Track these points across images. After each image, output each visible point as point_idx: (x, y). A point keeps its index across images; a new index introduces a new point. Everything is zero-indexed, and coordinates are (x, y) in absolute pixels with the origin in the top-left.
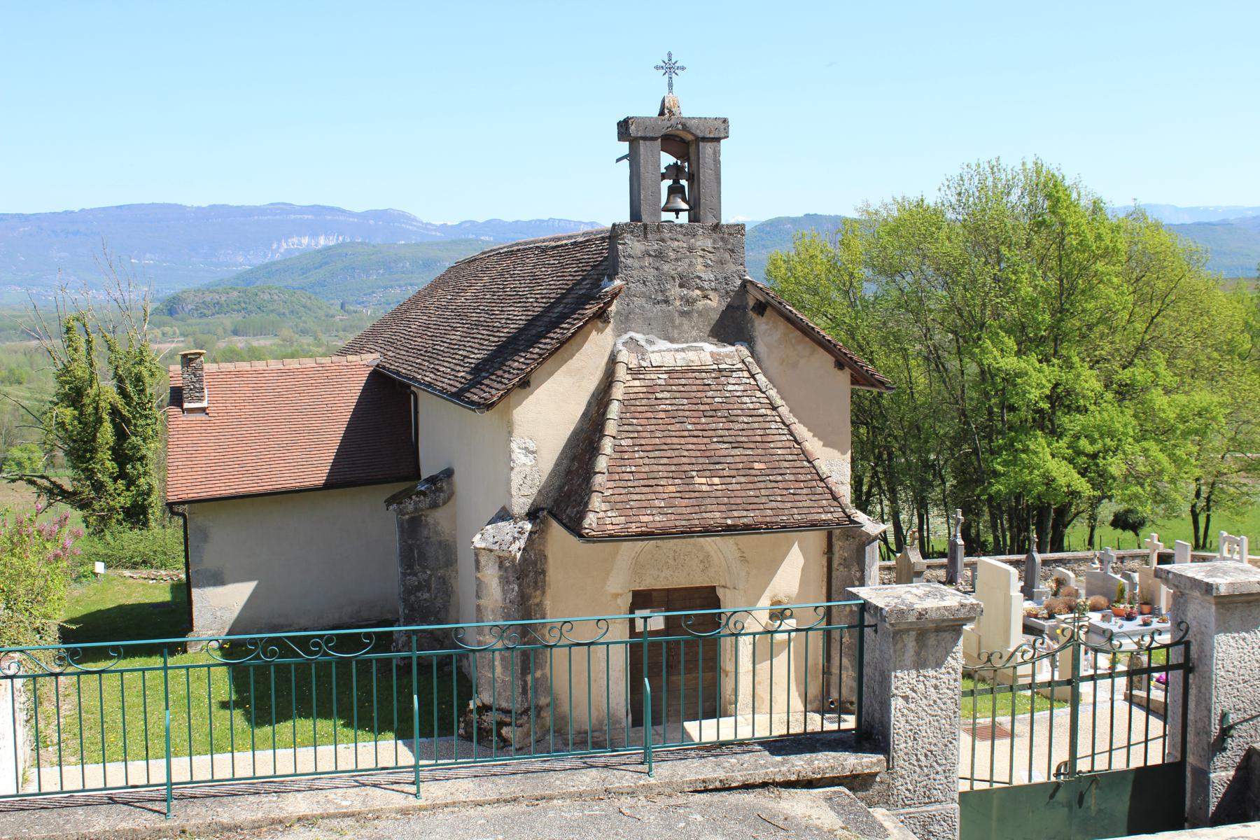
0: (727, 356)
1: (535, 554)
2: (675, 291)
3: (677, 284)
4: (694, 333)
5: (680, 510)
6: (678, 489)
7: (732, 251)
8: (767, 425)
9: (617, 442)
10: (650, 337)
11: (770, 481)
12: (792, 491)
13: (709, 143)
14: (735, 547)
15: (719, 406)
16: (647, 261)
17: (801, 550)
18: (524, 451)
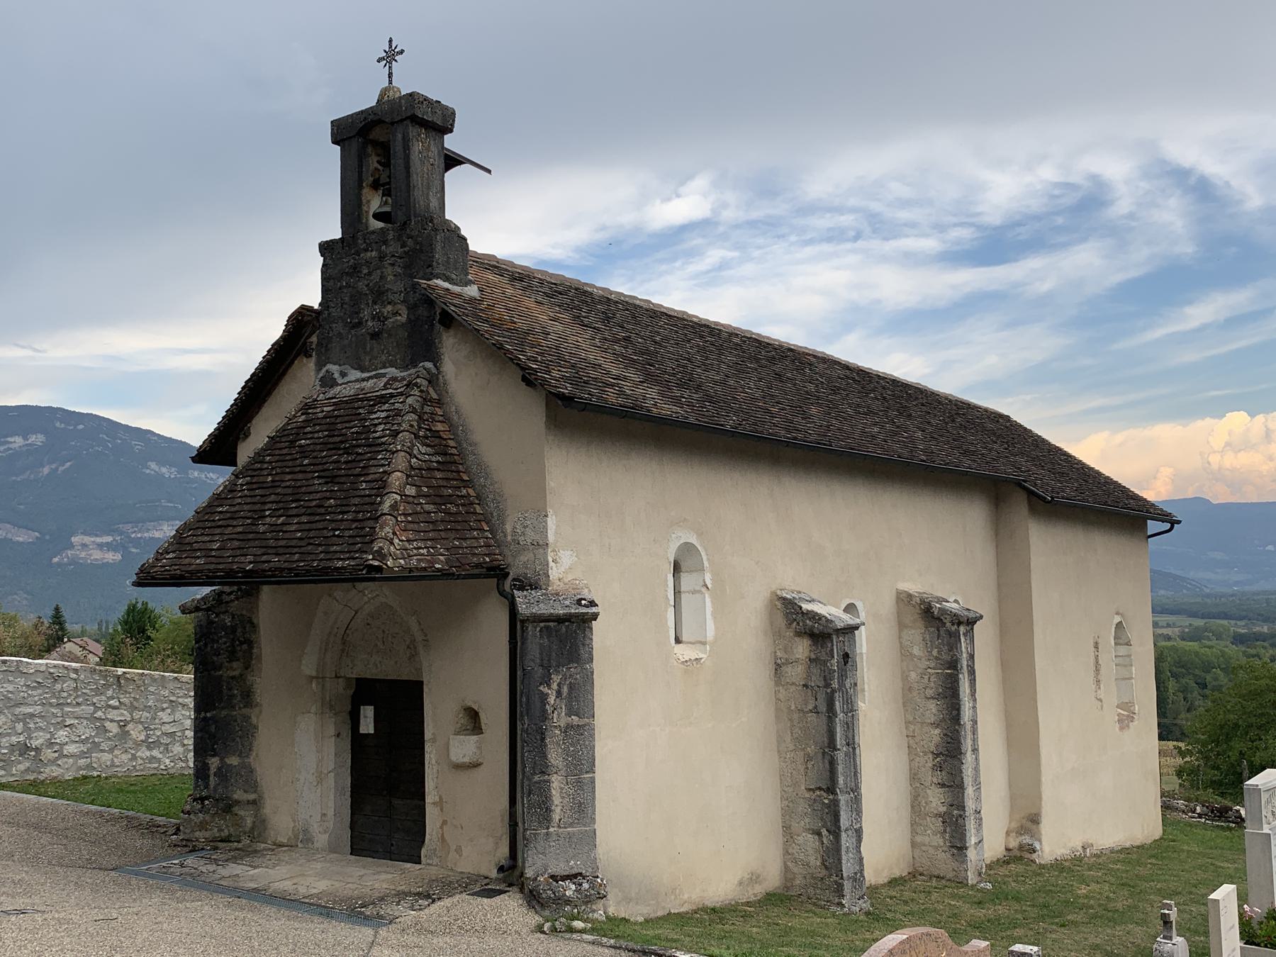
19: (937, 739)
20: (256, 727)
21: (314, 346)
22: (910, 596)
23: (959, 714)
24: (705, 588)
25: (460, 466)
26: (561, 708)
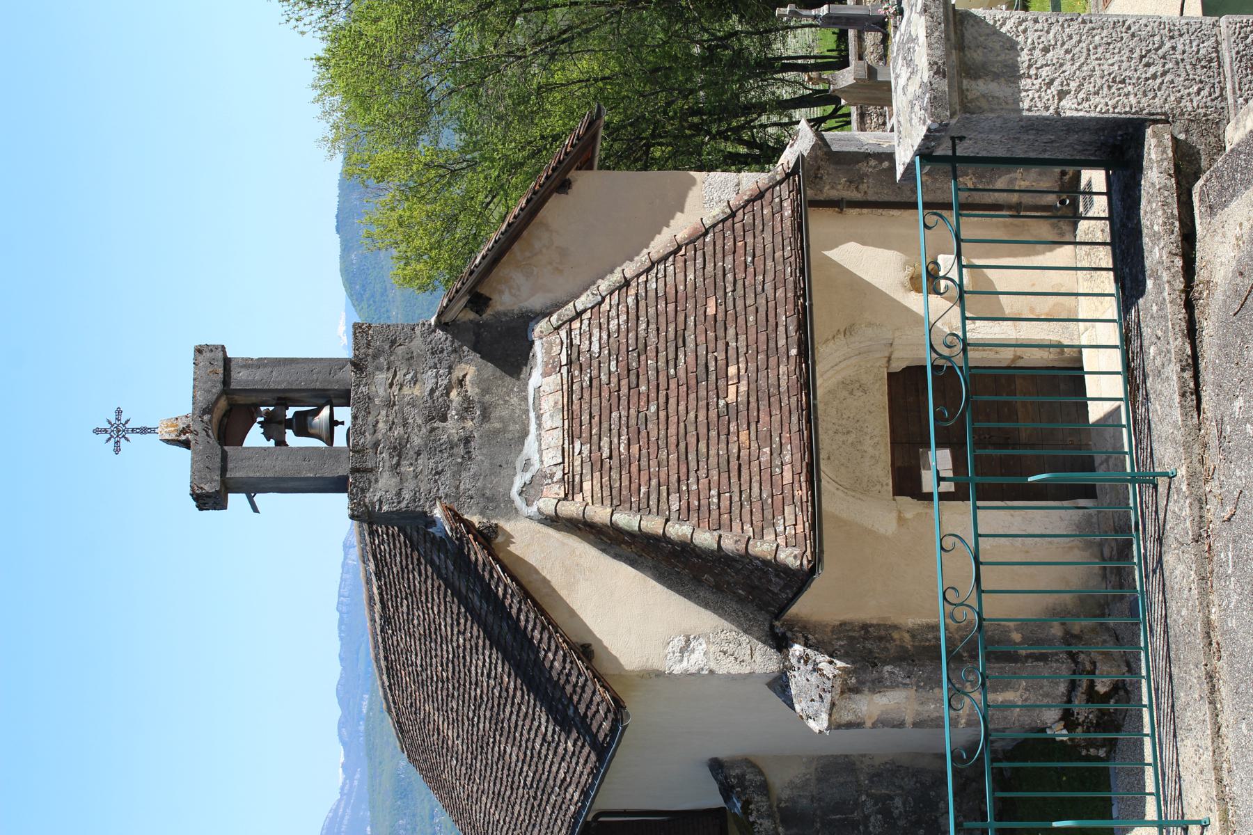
0: (548, 352)
1: (839, 639)
2: (452, 428)
4: (514, 400)
5: (776, 425)
6: (745, 426)
7: (393, 342)
8: (652, 294)
9: (674, 516)
10: (519, 464)
11: (734, 291)
12: (749, 259)
13: (232, 373)
14: (831, 344)
15: (623, 364)
16: (406, 469)
17: (836, 246)
18: (686, 654)
21: (485, 521)
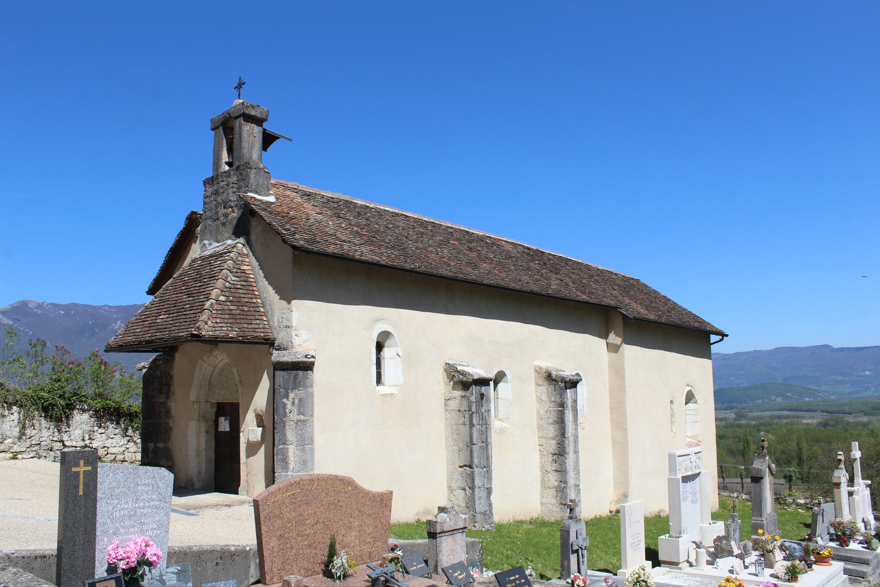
3: (223, 207)
19: (554, 446)
20: (171, 428)
22: (541, 368)
23: (564, 432)
24: (398, 356)
25: (255, 288)
26: (294, 411)
